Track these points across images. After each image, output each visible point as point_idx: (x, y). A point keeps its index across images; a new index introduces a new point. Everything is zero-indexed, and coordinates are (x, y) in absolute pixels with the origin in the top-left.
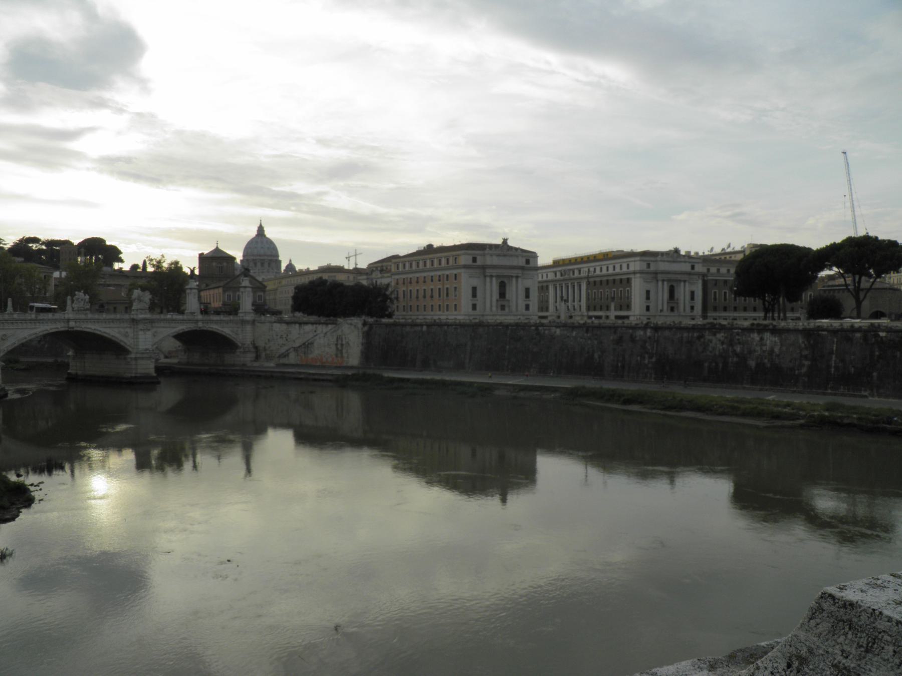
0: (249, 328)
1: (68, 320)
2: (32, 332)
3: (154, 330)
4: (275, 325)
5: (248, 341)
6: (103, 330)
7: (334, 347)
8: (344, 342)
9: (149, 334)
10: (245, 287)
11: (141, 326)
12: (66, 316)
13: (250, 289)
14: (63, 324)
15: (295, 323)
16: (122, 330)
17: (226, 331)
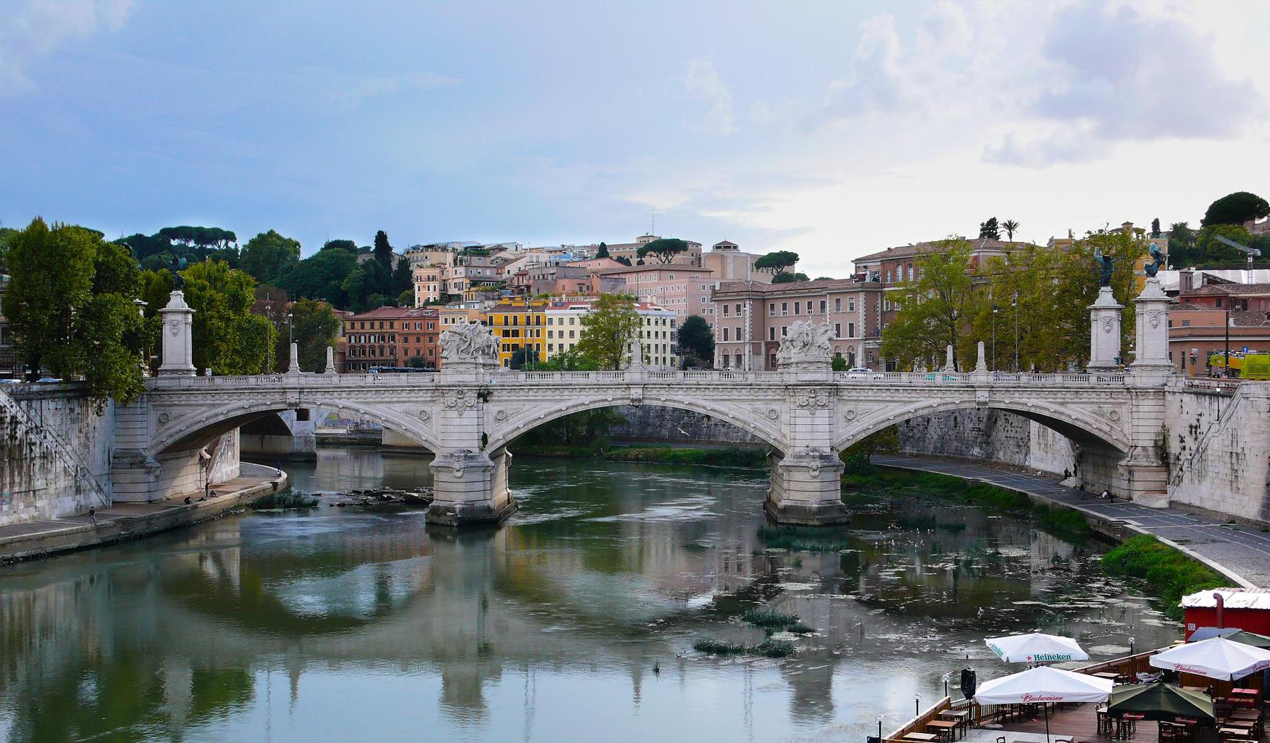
0: (1148, 405)
1: (628, 386)
2: (557, 407)
3: (851, 406)
4: (1186, 398)
5: (1146, 439)
6: (710, 405)
7: (1227, 459)
8: (1239, 451)
9: (822, 416)
10: (1143, 302)
11: (802, 398)
12: (627, 378)
13: (1161, 307)
14: (619, 393)
15: (1205, 394)
16: (759, 405)
17: (1079, 413)
